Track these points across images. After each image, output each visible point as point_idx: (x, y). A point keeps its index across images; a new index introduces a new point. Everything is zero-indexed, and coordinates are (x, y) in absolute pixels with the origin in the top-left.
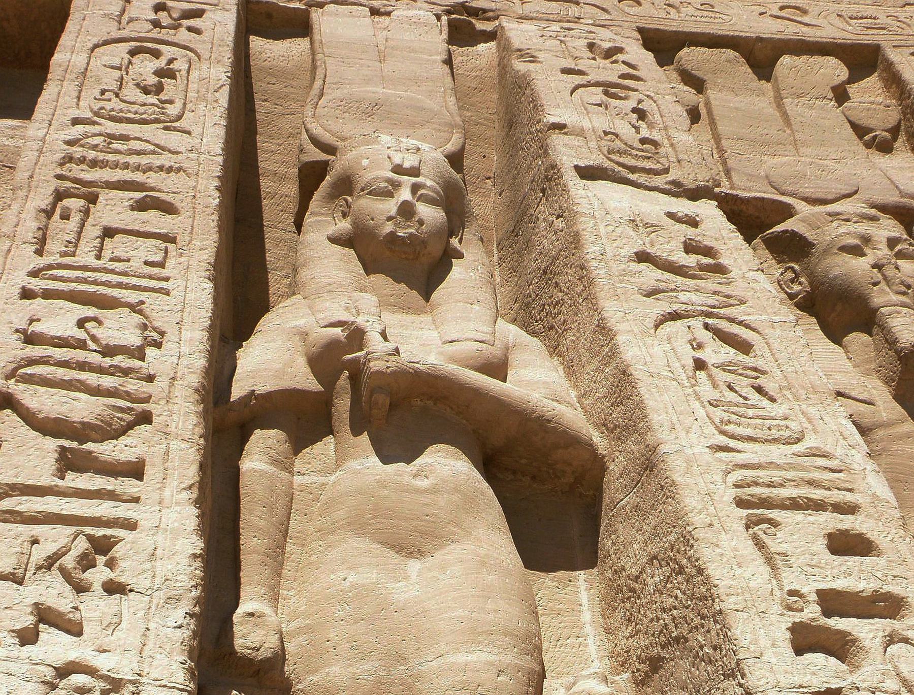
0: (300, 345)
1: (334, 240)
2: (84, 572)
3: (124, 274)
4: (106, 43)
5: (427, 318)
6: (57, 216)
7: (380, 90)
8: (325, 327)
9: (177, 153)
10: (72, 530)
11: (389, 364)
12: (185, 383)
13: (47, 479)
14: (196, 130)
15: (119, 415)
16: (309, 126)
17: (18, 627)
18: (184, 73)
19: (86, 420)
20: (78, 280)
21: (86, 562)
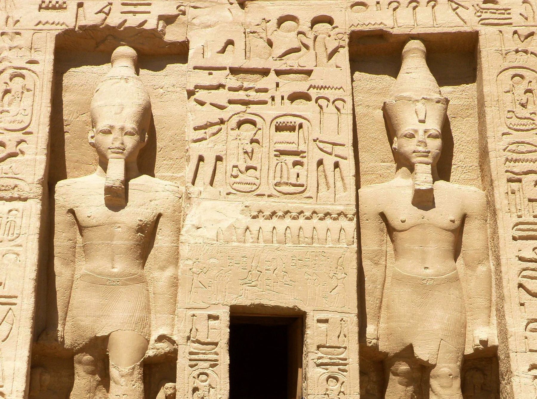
4: (501, 72)
20: (529, 230)
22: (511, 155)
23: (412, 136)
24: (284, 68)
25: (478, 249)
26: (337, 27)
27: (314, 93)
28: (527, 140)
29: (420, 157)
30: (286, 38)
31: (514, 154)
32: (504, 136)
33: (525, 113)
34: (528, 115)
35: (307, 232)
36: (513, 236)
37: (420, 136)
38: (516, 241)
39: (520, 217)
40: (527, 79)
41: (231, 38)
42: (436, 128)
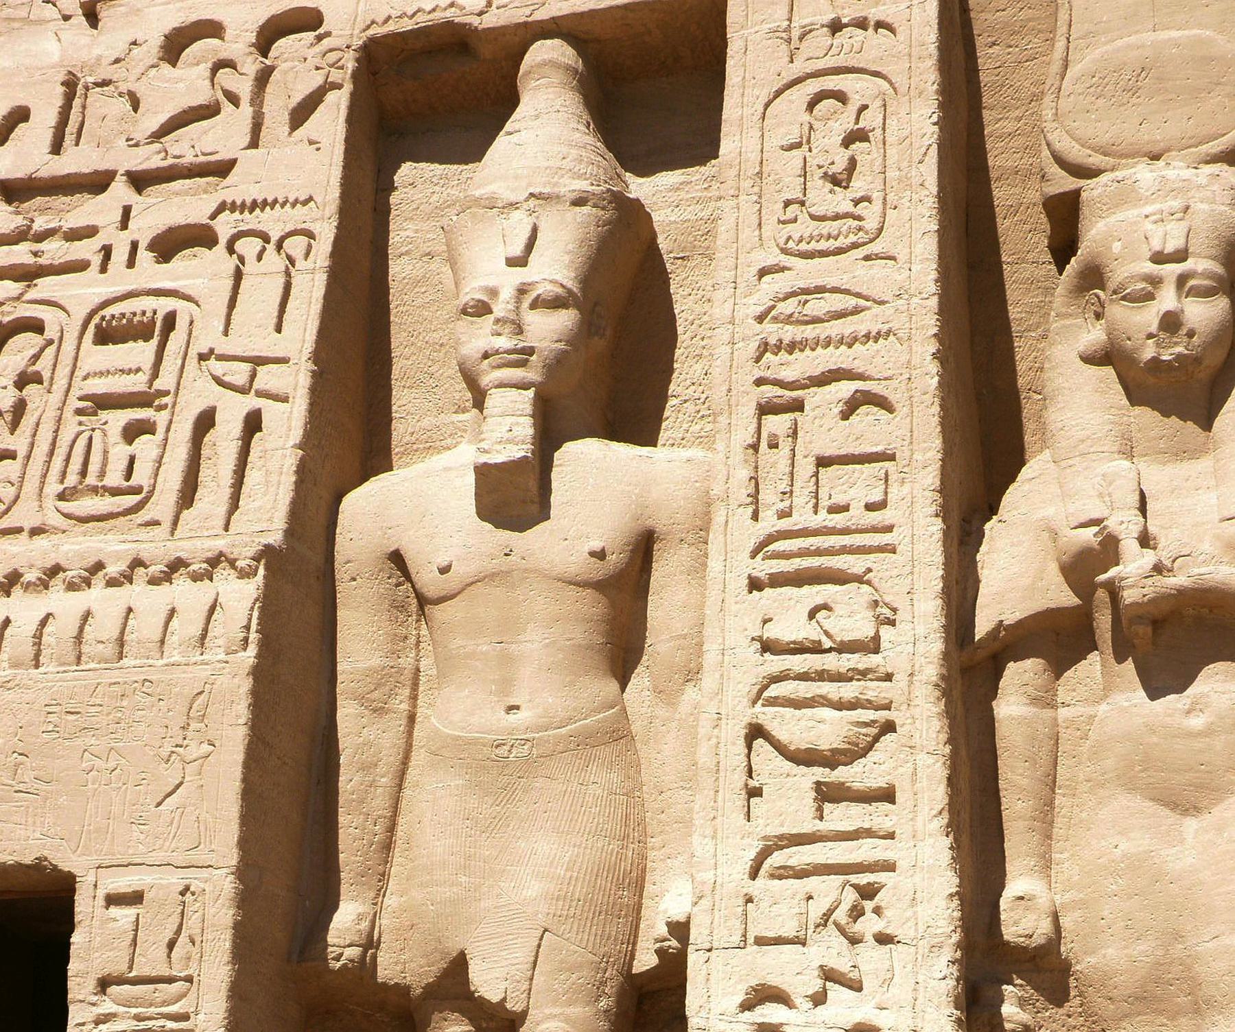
0: (1050, 544)
1: (1088, 359)
2: (855, 922)
3: (845, 531)
4: (778, 93)
5: (1204, 464)
6: (764, 445)
7: (1148, 37)
8: (1075, 528)
9: (882, 303)
10: (837, 880)
11: (1145, 591)
12: (924, 678)
13: (809, 825)
14: (902, 253)
15: (864, 731)
16: (1050, 137)
17: (810, 992)
18: (879, 132)
19: (834, 746)
21: (856, 913)
22: (773, 332)
23: (482, 309)
24: (156, 162)
25: (684, 637)
26: (328, 34)
27: (225, 226)
28: (831, 282)
29: (499, 367)
30: (188, 82)
31: (787, 327)
32: (766, 279)
33: (841, 201)
34: (847, 207)
35: (104, 628)
36: (750, 577)
37: (501, 308)
38: (760, 589)
39: (783, 514)
40: (855, 103)
41: (23, 103)
42: (559, 277)
